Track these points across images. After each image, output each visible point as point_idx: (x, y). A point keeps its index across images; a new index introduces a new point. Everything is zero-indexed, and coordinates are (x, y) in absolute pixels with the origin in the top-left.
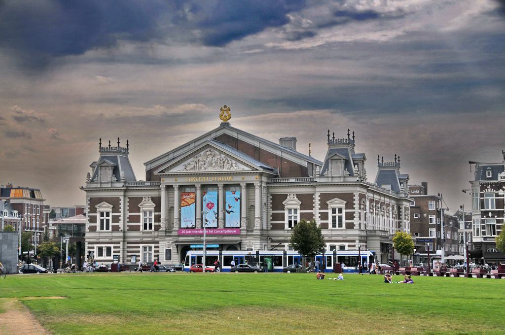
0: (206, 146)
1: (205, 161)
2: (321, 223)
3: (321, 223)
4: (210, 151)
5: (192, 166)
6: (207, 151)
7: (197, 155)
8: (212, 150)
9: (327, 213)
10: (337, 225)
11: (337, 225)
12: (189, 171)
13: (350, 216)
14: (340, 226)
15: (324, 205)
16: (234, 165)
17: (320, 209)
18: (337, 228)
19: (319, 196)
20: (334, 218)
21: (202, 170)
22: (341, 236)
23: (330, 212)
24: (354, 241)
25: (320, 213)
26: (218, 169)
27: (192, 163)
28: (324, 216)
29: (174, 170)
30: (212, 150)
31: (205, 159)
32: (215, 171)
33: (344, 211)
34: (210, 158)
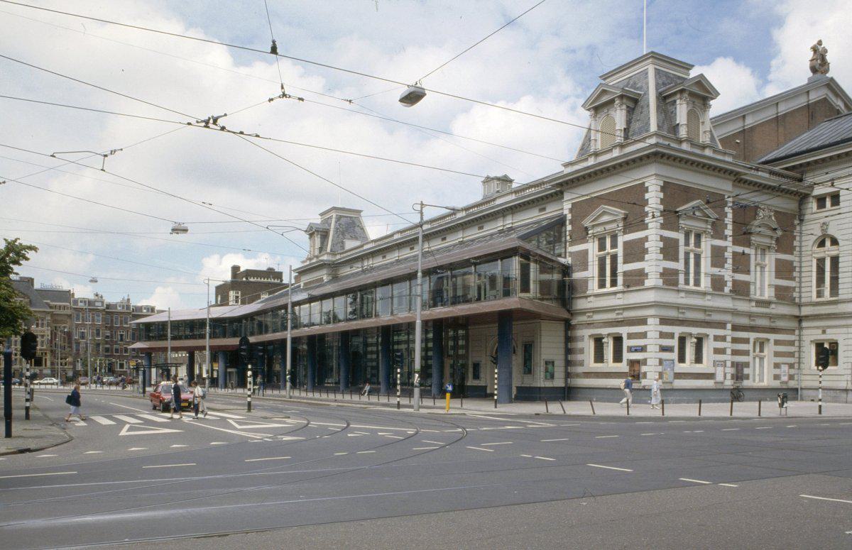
2: (664, 269)
3: (664, 269)
9: (677, 241)
10: (692, 281)
11: (692, 281)
13: (718, 257)
14: (697, 283)
15: (671, 217)
17: (663, 227)
18: (691, 286)
19: (663, 189)
20: (687, 254)
22: (704, 310)
23: (680, 237)
24: (722, 325)
25: (662, 238)
28: (669, 250)
33: (707, 244)
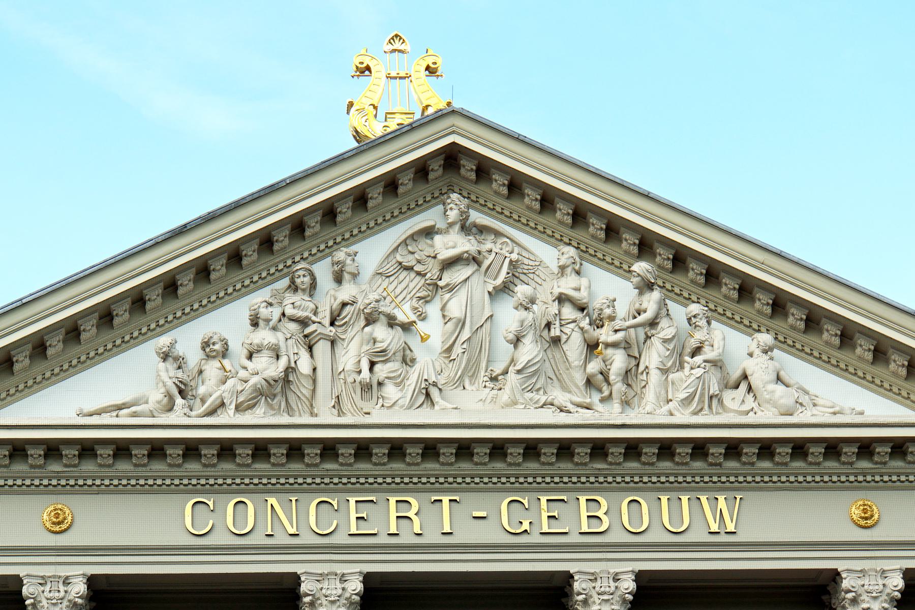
0: (421, 169)
1: (406, 327)
4: (466, 228)
5: (275, 370)
6: (429, 232)
7: (323, 270)
8: (477, 217)
12: (228, 416)
16: (760, 370)
21: (394, 413)
26: (560, 410)
27: (264, 336)
29: (59, 406)
30: (477, 217)
31: (404, 314)
32: (548, 416)
34: (468, 294)
